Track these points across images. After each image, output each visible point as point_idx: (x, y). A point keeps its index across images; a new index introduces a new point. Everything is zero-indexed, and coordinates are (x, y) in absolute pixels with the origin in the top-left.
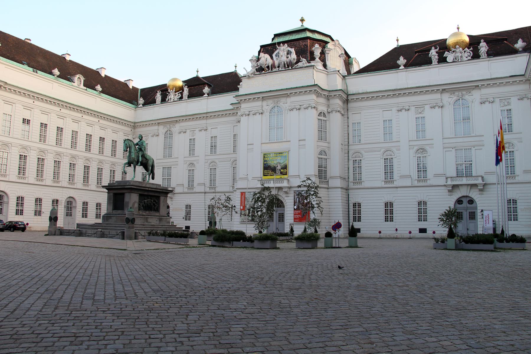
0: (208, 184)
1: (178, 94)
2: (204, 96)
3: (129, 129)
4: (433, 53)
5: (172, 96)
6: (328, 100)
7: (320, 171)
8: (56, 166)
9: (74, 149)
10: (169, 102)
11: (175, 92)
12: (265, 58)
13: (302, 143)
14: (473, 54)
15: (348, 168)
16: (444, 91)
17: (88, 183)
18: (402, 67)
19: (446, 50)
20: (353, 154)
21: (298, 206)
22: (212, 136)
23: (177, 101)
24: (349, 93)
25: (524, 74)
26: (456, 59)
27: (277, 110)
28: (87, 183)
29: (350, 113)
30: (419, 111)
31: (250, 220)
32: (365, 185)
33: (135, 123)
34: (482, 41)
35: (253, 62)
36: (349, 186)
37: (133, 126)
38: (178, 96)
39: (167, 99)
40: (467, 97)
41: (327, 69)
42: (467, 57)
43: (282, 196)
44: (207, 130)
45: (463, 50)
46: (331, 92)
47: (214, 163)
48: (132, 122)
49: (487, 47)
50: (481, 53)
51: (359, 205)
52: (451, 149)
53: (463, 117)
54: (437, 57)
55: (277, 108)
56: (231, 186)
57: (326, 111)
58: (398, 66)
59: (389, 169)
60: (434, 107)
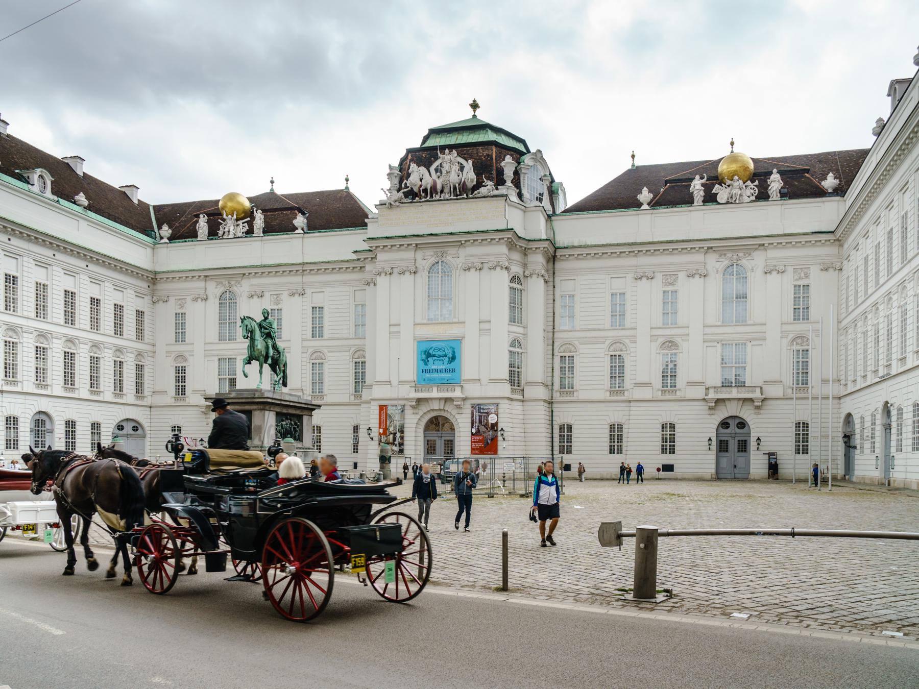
0: (308, 389)
1: (243, 223)
2: (297, 232)
3: (145, 285)
4: (697, 186)
5: (230, 226)
6: (525, 255)
7: (511, 373)
8: (8, 351)
9: (42, 319)
10: (225, 237)
11: (237, 220)
12: (419, 176)
13: (485, 326)
14: (758, 189)
15: (553, 369)
16: (710, 250)
17: (74, 385)
18: (645, 207)
19: (715, 181)
20: (561, 346)
21: (478, 428)
22: (314, 305)
23: (241, 237)
24: (557, 246)
25: (833, 230)
26: (731, 197)
27: (442, 269)
28: (71, 384)
29: (556, 279)
30: (669, 280)
32: (582, 395)
33: (156, 273)
34: (775, 171)
35: (393, 178)
36: (554, 398)
37: (152, 279)
38: (243, 228)
39: (220, 233)
40: (744, 262)
41: (523, 201)
42: (749, 197)
43: (451, 412)
44: (305, 296)
45: (744, 183)
46: (531, 243)
47: (319, 354)
48: (151, 272)
49: (781, 181)
50: (772, 191)
51: (570, 428)
53: (736, 294)
54: (702, 193)
56: (352, 394)
57: (522, 274)
58: (638, 205)
59: (617, 371)
60: (693, 276)
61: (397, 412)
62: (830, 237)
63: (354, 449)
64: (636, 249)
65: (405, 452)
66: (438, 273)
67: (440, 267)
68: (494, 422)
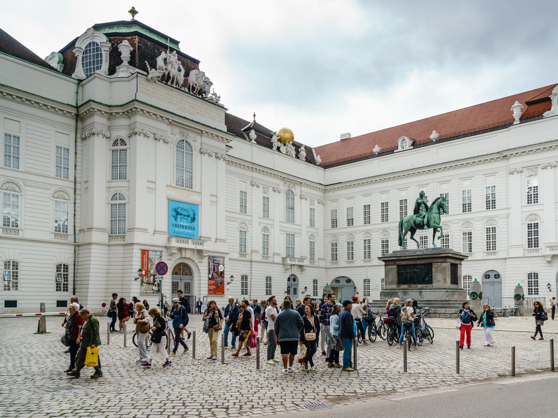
18: (253, 141)
31: (156, 291)
52: (283, 233)
61: (157, 257)
62: (323, 187)
63: (57, 287)
64: (255, 167)
68: (222, 270)
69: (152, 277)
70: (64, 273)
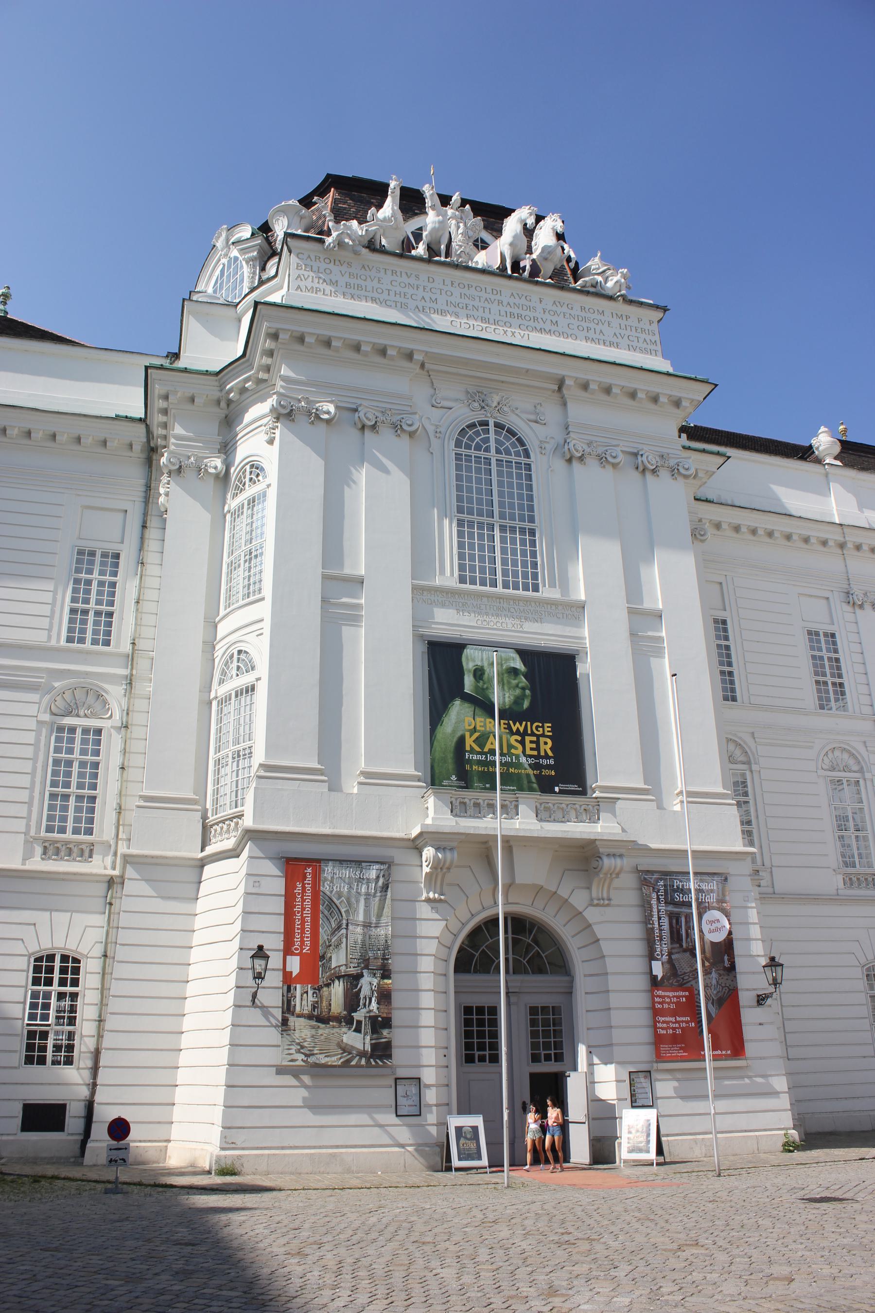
21: (670, 961)
31: (362, 1054)
55: (496, 433)
65: (399, 1056)
66: (487, 450)
67: (492, 436)
69: (338, 990)
70: (56, 981)
